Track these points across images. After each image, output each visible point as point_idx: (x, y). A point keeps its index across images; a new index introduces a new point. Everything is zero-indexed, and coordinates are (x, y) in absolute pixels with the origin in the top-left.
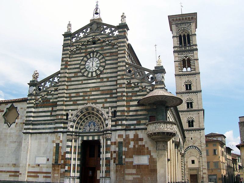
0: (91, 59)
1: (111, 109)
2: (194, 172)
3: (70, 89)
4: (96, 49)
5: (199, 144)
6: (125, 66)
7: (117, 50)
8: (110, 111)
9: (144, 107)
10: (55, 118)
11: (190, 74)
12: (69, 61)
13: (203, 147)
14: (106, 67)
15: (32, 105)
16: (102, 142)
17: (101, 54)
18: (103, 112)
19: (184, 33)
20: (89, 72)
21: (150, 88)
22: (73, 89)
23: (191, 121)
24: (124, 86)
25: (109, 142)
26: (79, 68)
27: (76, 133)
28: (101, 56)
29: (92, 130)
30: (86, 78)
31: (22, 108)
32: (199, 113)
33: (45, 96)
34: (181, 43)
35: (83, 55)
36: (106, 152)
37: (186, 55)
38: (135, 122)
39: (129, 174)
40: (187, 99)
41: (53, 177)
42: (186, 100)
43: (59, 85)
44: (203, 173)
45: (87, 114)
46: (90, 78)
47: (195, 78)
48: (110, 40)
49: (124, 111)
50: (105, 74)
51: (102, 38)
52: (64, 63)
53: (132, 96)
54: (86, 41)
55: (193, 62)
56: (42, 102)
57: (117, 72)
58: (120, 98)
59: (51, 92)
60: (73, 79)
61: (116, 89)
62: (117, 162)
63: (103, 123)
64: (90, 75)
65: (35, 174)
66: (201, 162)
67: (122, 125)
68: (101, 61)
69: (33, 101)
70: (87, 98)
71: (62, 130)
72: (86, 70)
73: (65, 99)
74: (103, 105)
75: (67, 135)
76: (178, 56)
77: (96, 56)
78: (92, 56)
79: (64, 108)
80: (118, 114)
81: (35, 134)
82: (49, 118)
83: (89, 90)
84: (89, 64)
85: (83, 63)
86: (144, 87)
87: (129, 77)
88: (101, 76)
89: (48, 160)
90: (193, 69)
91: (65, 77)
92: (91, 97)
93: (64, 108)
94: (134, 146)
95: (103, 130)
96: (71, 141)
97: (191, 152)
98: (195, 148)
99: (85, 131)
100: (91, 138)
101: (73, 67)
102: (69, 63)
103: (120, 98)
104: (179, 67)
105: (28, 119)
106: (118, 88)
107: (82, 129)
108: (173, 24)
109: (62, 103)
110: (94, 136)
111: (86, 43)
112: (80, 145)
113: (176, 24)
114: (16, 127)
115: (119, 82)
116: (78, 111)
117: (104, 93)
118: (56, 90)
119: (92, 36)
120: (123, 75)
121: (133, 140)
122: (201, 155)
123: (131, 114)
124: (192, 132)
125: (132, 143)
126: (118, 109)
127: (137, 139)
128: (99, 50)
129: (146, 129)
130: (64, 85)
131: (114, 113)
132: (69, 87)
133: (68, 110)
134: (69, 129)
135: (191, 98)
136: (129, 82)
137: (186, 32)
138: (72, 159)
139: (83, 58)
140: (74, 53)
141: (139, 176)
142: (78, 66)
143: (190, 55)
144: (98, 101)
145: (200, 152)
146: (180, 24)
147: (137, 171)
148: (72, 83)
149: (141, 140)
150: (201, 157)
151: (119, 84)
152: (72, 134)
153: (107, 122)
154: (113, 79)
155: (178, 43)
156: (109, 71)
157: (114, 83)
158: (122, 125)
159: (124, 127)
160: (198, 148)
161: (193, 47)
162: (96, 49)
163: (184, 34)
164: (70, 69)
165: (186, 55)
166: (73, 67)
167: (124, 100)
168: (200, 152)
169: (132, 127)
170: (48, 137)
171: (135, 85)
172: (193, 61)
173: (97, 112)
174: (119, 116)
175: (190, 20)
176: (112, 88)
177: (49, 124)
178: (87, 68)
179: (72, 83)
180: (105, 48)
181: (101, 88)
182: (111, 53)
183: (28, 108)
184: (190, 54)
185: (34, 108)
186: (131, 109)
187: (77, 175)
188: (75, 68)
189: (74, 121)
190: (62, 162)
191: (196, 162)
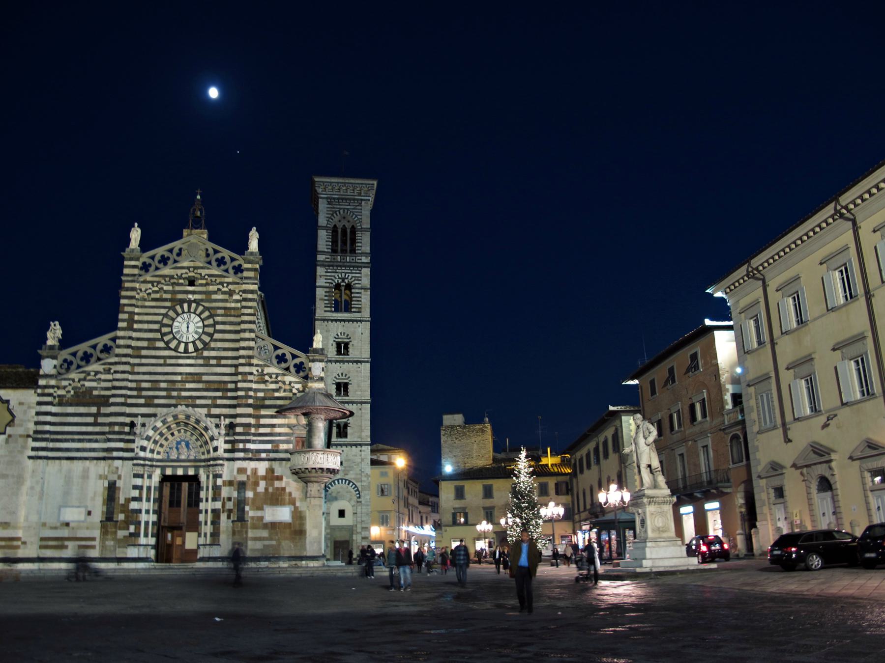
0: (185, 315)
1: (224, 420)
2: (341, 536)
3: (138, 373)
4: (197, 297)
5: (357, 474)
6: (253, 340)
7: (239, 305)
8: (223, 423)
9: (287, 420)
10: (106, 429)
11: (349, 321)
12: (139, 314)
13: (364, 481)
14: (216, 336)
15: (49, 399)
16: (203, 478)
17: (206, 309)
18: (209, 423)
19: (344, 222)
20: (180, 342)
21: (299, 386)
22: (144, 374)
23: (342, 425)
24: (250, 378)
25: (219, 482)
26: (159, 331)
27: (151, 460)
28: (207, 314)
29: (183, 457)
30: (173, 353)
31: (21, 404)
32: (360, 409)
33: (82, 383)
34: (334, 242)
35: (168, 304)
36: (214, 499)
37: (343, 274)
38: (269, 446)
39: (255, 539)
40: (338, 375)
41: (103, 547)
42: (335, 377)
43: (116, 363)
44: (363, 538)
45: (175, 425)
46: (183, 355)
47: (360, 329)
48: (226, 283)
49: (249, 425)
50: (213, 349)
51: (210, 276)
52: (125, 316)
53: (264, 399)
54: (176, 277)
55: (357, 293)
56: (72, 392)
57: (237, 349)
58: (243, 401)
59: (95, 375)
60: (144, 352)
61: (236, 382)
62: (234, 517)
63: (206, 443)
64: (182, 348)
65: (60, 543)
66: (359, 515)
67: (245, 450)
68: (206, 323)
69: (51, 391)
70: (175, 394)
71: (121, 454)
72: (174, 338)
73: (129, 393)
74: (209, 411)
75: (134, 465)
76: (325, 274)
77: (196, 309)
78: (186, 309)
79: (128, 410)
80: (239, 430)
81: (57, 462)
82: (90, 429)
83: (179, 378)
84: (180, 325)
85: (166, 321)
86: (287, 383)
87: (261, 363)
88: (206, 353)
89: (89, 513)
90: (357, 310)
91: (129, 347)
92: (184, 394)
93: (128, 410)
94: (266, 489)
95: (206, 456)
96: (142, 476)
97: (339, 492)
98: (348, 484)
99: (168, 456)
100: (180, 472)
101: (145, 326)
102: (136, 318)
103: (243, 401)
104: (326, 300)
105: (40, 428)
106: (239, 381)
107: (162, 454)
108: (321, 198)
109: (121, 400)
110: (188, 467)
111: (175, 281)
112: (157, 485)
113: (327, 198)
114: (7, 441)
115: (241, 369)
116: (157, 418)
117: (210, 386)
118: (108, 371)
119: (188, 268)
120: (251, 357)
121: (264, 478)
122: (359, 500)
123: (262, 430)
124: (344, 448)
125: (262, 484)
126: (239, 420)
127: (271, 476)
128: (202, 300)
129: (289, 460)
130: (125, 363)
131: (231, 427)
132: (137, 369)
133: (136, 415)
134: (137, 454)
135: (346, 375)
136: (260, 371)
137: (349, 221)
138: (143, 512)
139: (168, 311)
140: (146, 297)
141: (274, 543)
142: (156, 327)
143: (350, 277)
144: (198, 402)
145: (358, 492)
146: (338, 199)
147: (270, 534)
148: (144, 361)
149: (280, 478)
150: (358, 504)
151: (241, 373)
152: (142, 462)
153: (215, 443)
154: (229, 362)
155: (328, 243)
156: (219, 345)
157: (232, 370)
158: (245, 450)
159: (250, 455)
160: (354, 484)
161: (360, 258)
162: (197, 297)
163: (344, 226)
164: (140, 330)
165: (343, 274)
166: (145, 326)
167: (249, 406)
168: (358, 492)
169: (263, 455)
170: (88, 468)
171: (271, 377)
172: (357, 291)
173: (195, 423)
174: (239, 434)
175: (360, 194)
176: (226, 378)
177: (90, 441)
178: (176, 333)
179: (144, 361)
180: (214, 297)
181: (205, 378)
182: (225, 308)
183: (40, 403)
184: (354, 275)
185: (54, 405)
186: (263, 421)
187: (152, 541)
188: (151, 331)
189: (148, 438)
190: (121, 517)
191: (347, 514)
